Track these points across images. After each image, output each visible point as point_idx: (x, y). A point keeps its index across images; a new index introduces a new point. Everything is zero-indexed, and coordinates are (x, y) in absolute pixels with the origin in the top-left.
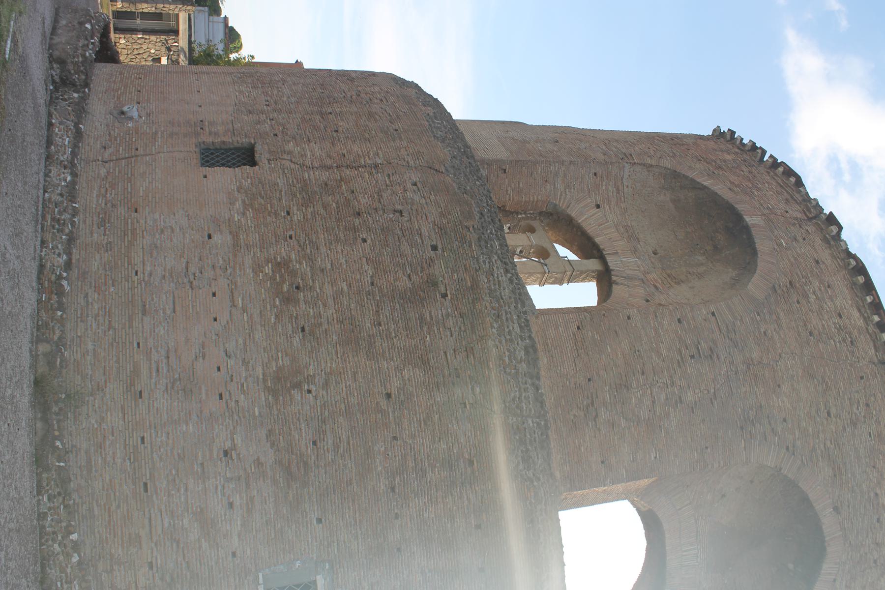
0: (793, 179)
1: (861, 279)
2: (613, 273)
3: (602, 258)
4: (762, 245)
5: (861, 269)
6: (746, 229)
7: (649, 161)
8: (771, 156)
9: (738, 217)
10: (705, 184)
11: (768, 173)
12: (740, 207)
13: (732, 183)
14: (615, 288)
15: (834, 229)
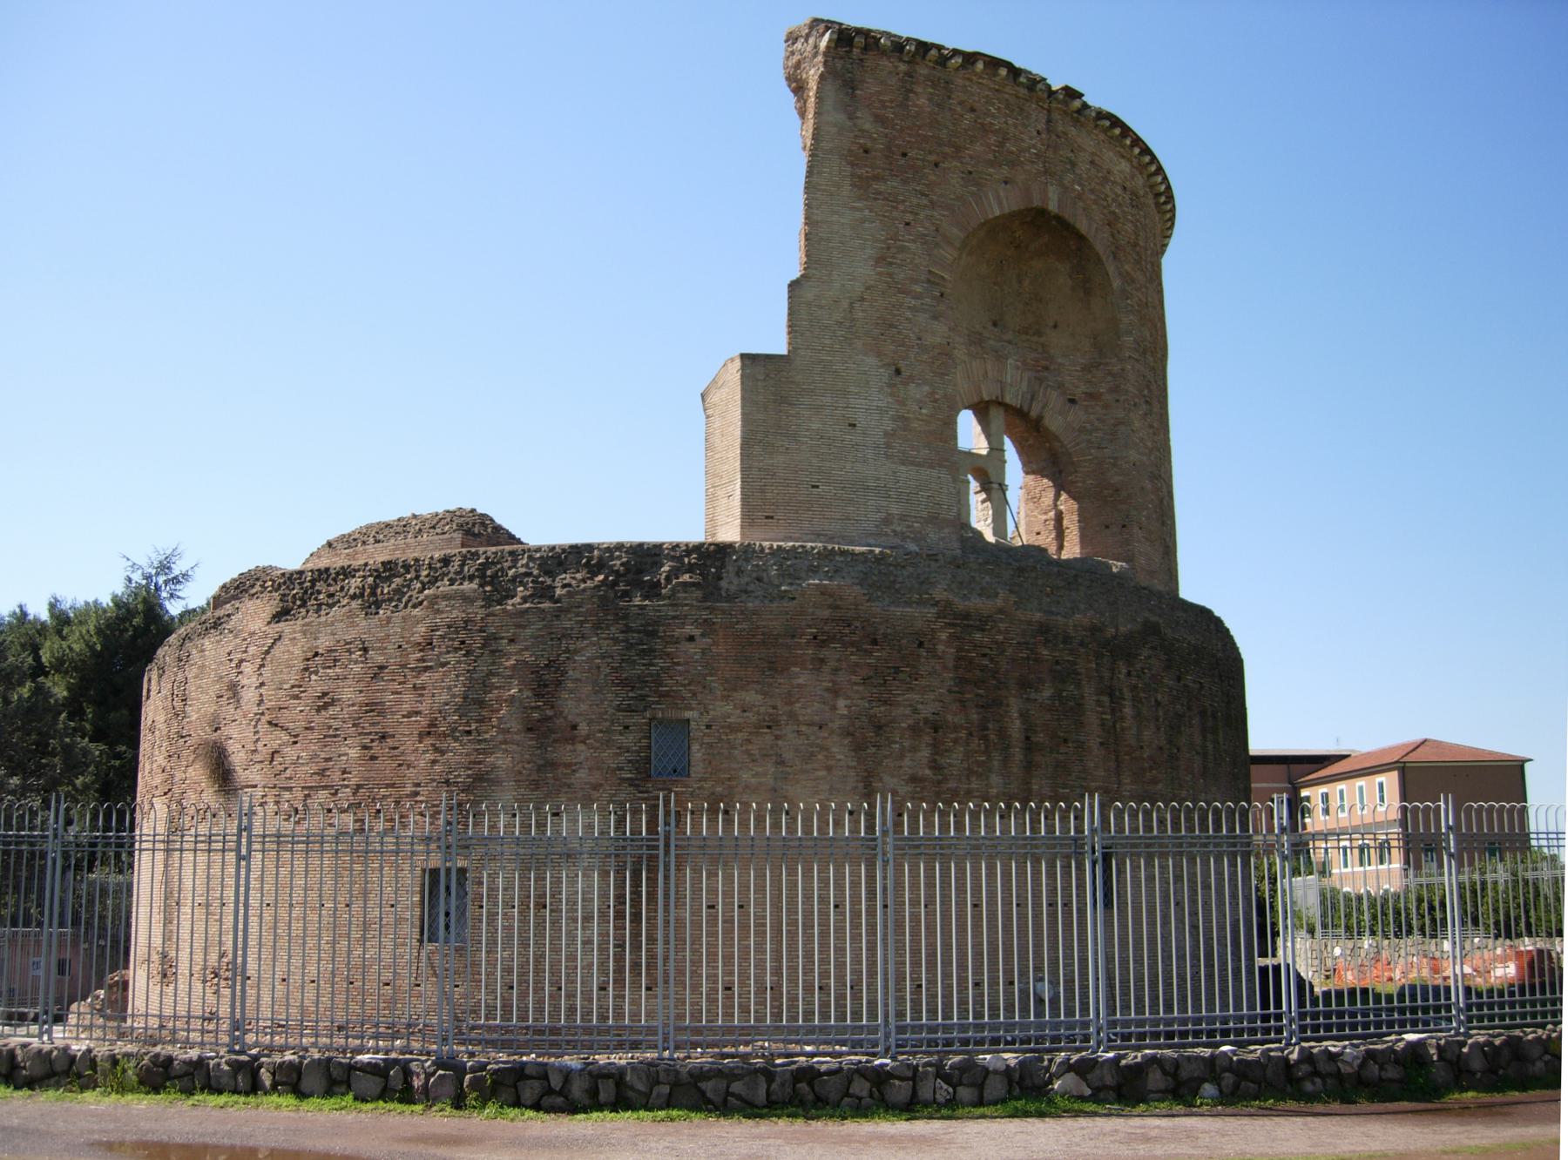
0: (1003, 72)
1: (1117, 131)
2: (1025, 409)
3: (1000, 403)
4: (1082, 225)
5: (1115, 121)
6: (1058, 218)
7: (948, 254)
8: (956, 52)
9: (1042, 213)
10: (997, 213)
11: (970, 80)
12: (1036, 203)
13: (992, 164)
14: (1047, 422)
15: (1077, 104)
